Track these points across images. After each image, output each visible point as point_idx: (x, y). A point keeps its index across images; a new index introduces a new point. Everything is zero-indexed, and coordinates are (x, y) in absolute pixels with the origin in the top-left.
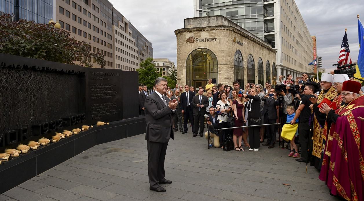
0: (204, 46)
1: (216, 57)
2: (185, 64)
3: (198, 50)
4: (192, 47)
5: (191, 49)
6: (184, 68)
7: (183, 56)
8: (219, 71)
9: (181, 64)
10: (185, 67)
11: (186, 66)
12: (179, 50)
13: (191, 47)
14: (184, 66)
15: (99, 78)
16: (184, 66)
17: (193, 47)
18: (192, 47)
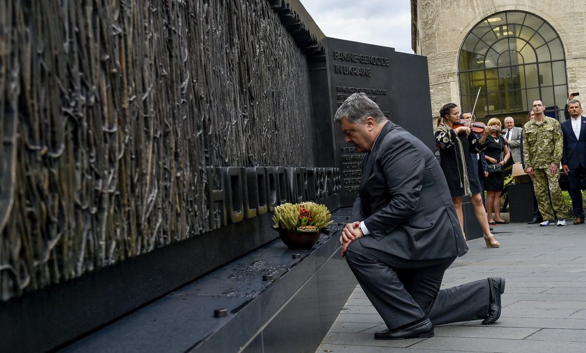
0: (516, 2)
1: (558, 37)
2: (455, 68)
3: (490, 20)
4: (474, 9)
5: (471, 17)
6: (451, 79)
7: (446, 41)
8: (571, 81)
9: (440, 67)
10: (456, 78)
11: (459, 74)
12: (433, 20)
13: (470, 9)
14: (450, 74)
15: (350, 69)
16: (450, 74)
17: (477, 12)
18: (474, 9)
